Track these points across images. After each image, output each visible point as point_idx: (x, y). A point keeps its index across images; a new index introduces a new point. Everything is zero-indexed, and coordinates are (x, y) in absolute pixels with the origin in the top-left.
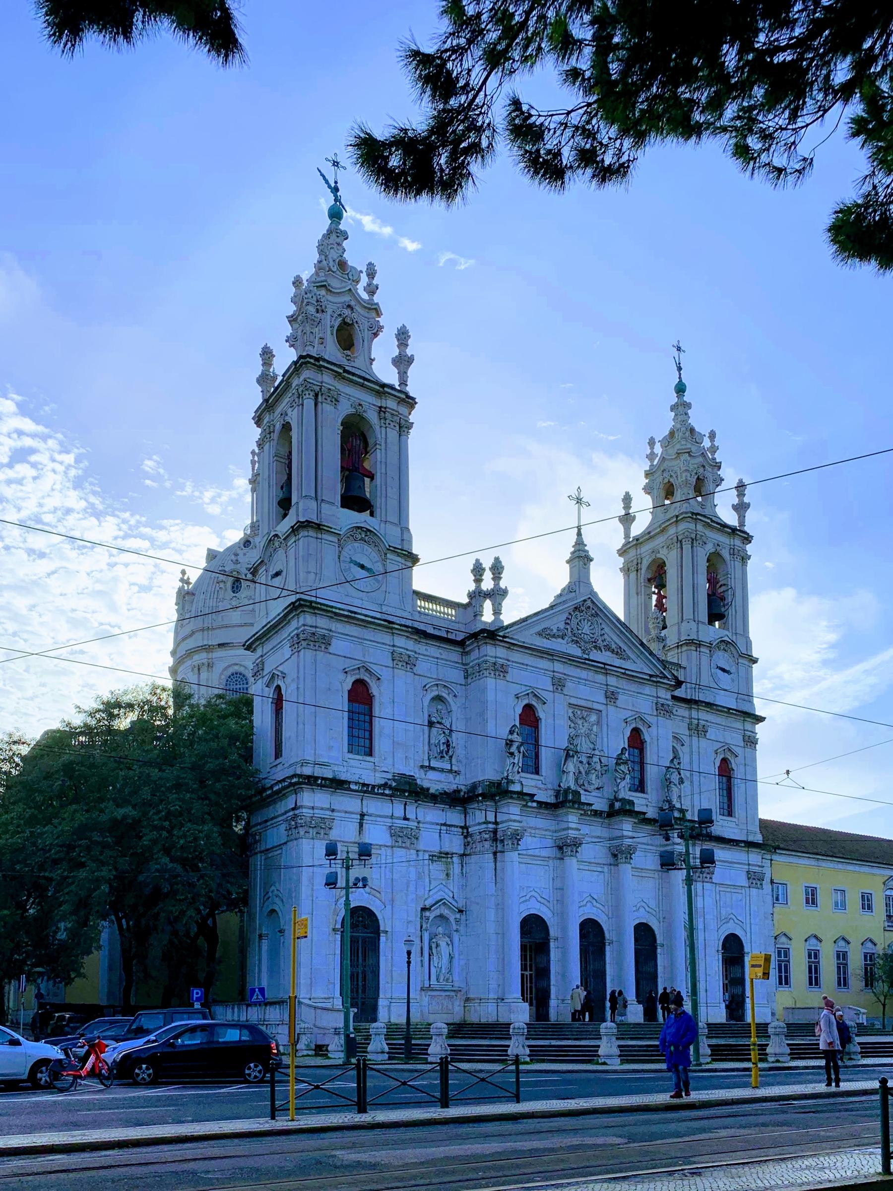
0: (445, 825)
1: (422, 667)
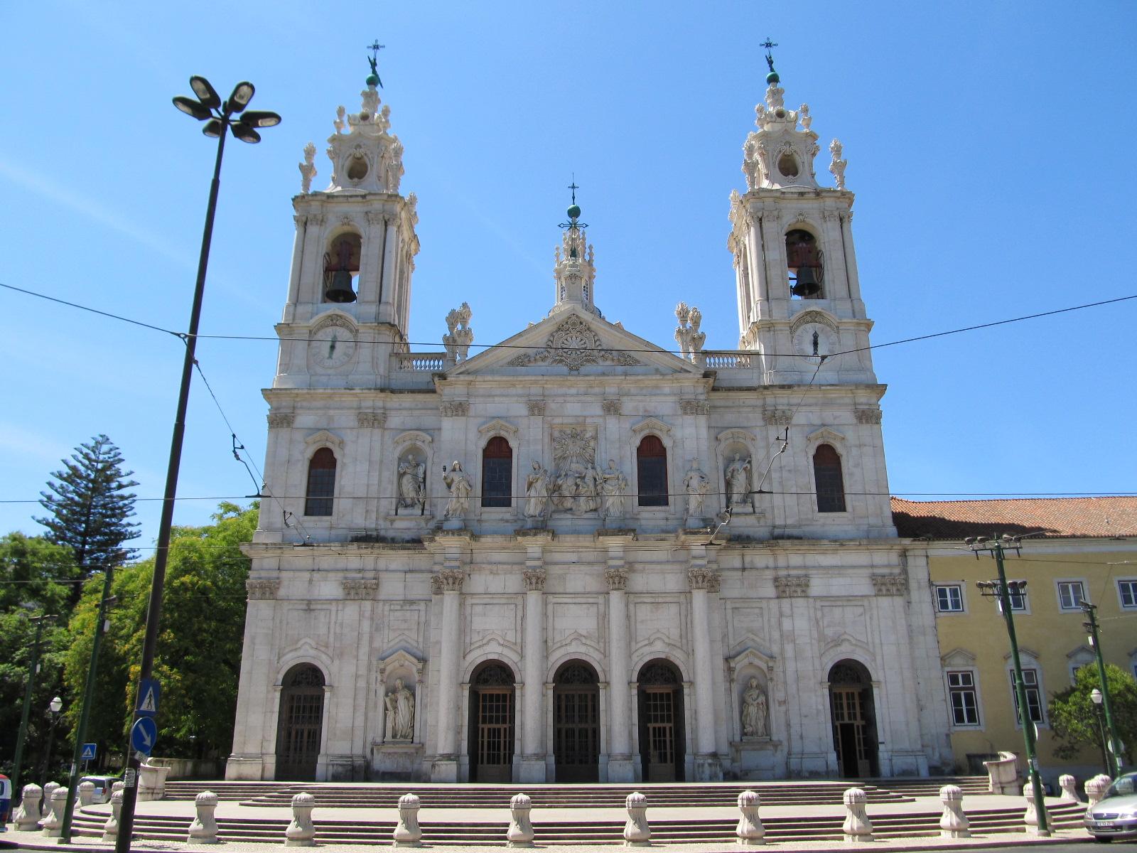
0: (411, 571)
1: (395, 421)
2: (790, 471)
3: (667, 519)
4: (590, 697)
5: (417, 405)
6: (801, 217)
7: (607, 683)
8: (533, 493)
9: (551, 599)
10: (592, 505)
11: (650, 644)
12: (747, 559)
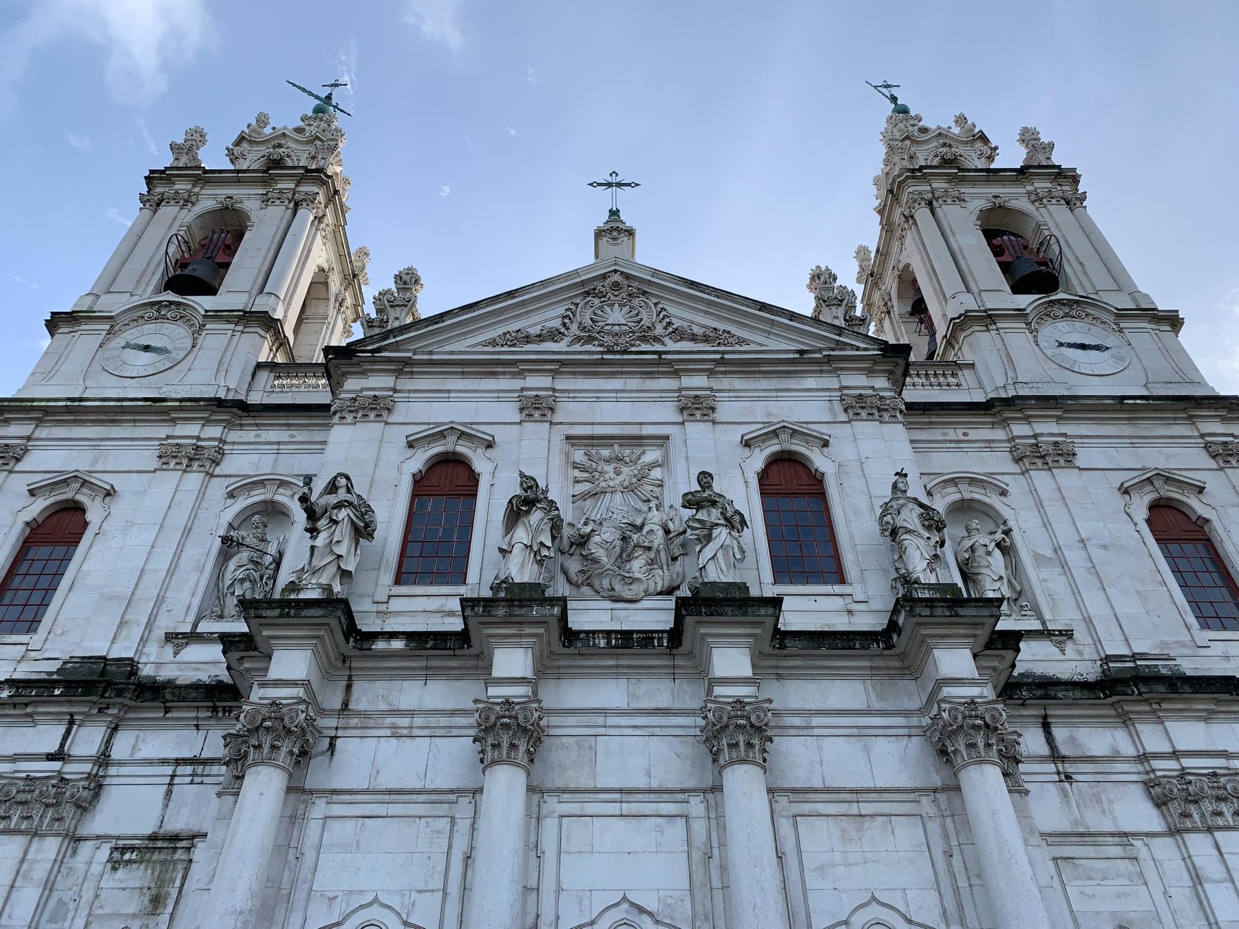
1: (239, 463)
2: (1105, 547)
3: (850, 612)
5: (293, 436)
6: (997, 201)
8: (521, 534)
9: (553, 805)
10: (661, 579)
12: (1060, 733)
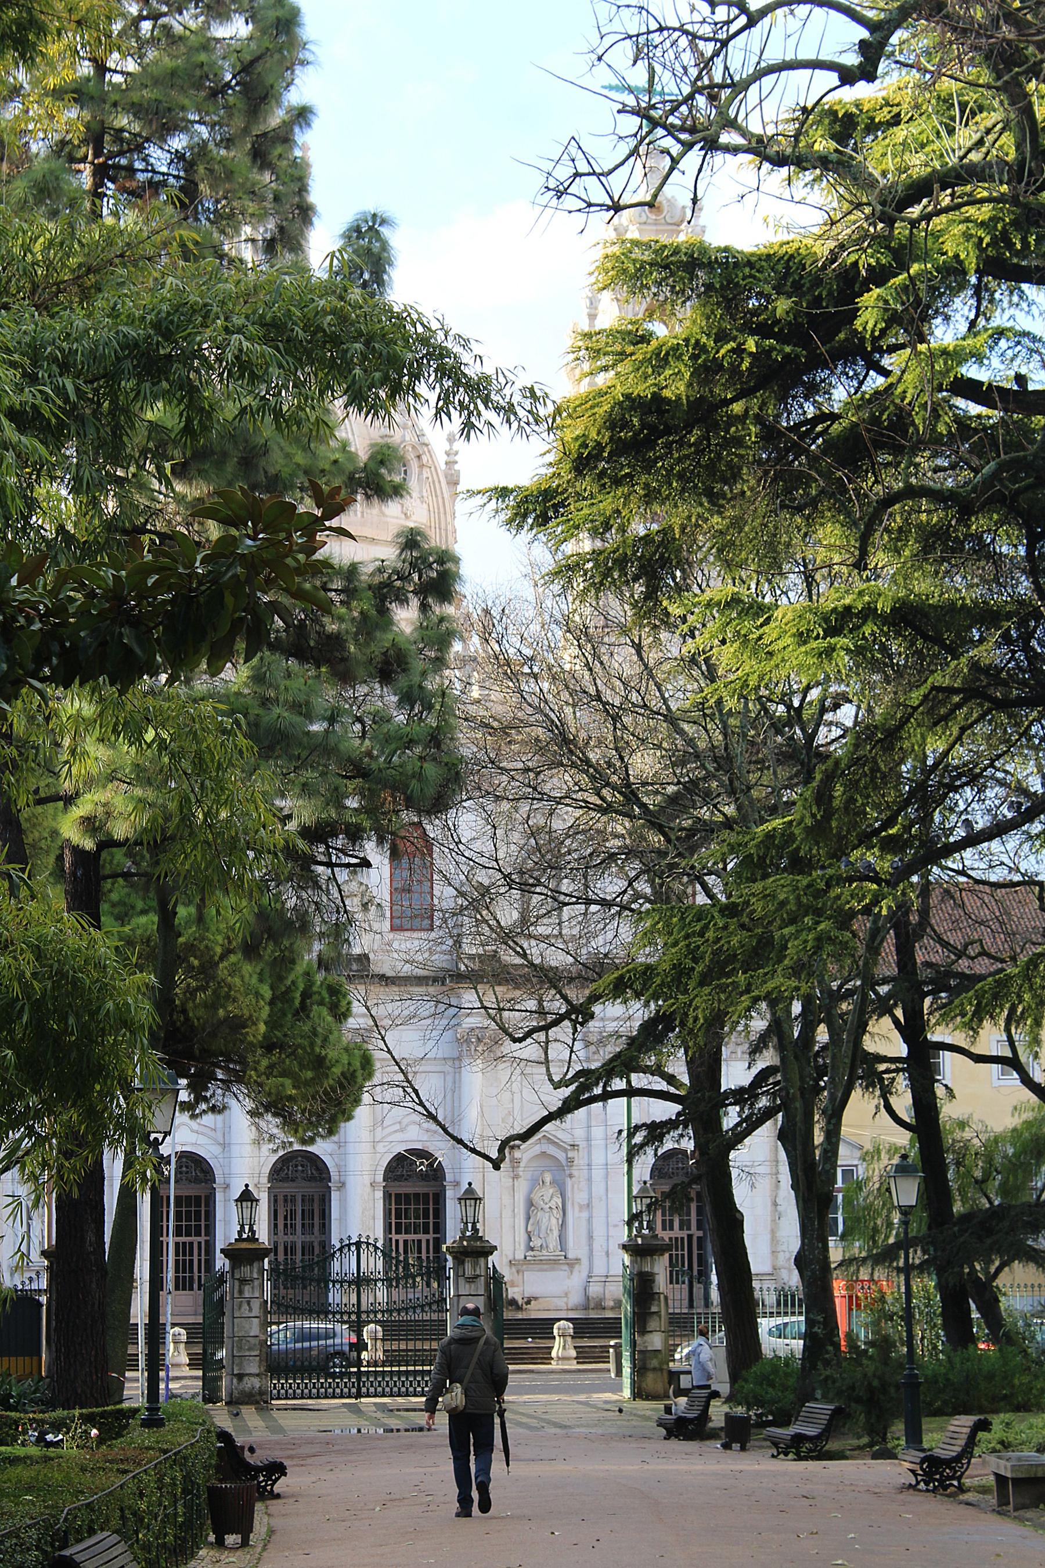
4: (316, 1198)
7: (342, 1185)
11: (402, 1130)
